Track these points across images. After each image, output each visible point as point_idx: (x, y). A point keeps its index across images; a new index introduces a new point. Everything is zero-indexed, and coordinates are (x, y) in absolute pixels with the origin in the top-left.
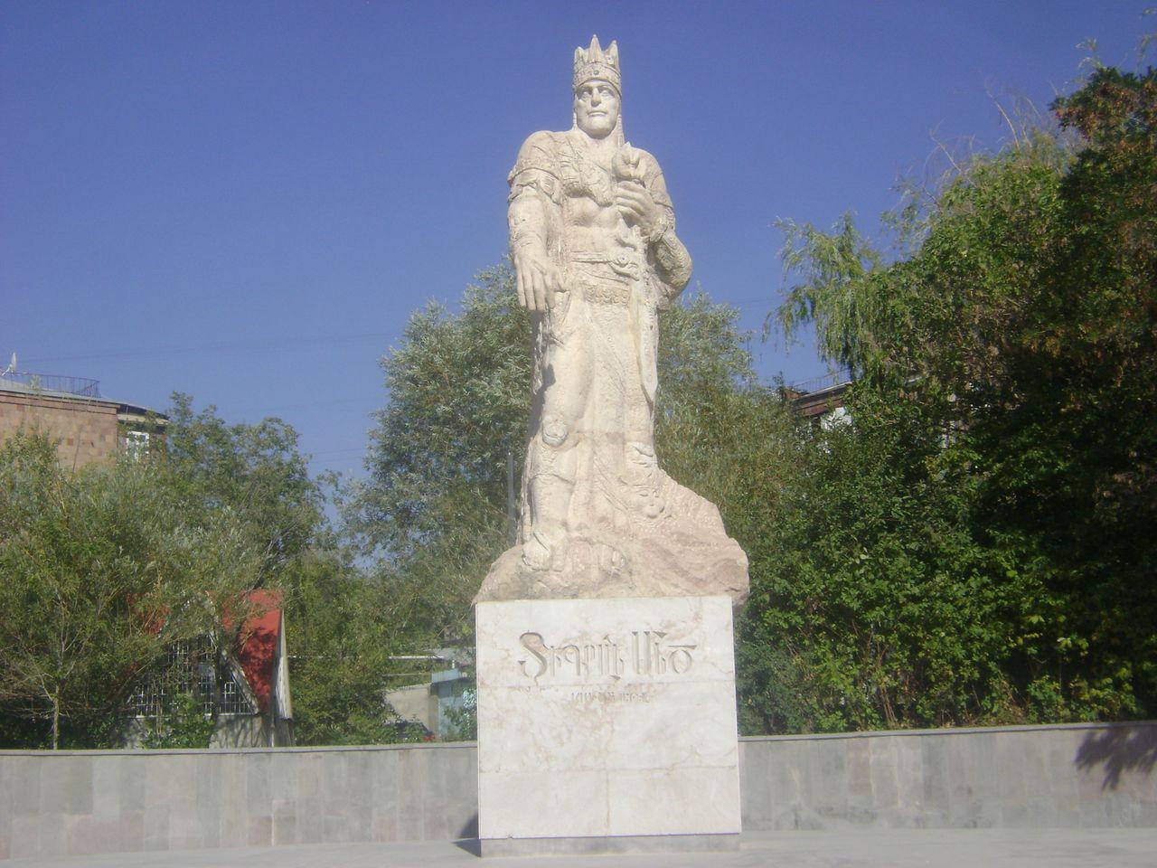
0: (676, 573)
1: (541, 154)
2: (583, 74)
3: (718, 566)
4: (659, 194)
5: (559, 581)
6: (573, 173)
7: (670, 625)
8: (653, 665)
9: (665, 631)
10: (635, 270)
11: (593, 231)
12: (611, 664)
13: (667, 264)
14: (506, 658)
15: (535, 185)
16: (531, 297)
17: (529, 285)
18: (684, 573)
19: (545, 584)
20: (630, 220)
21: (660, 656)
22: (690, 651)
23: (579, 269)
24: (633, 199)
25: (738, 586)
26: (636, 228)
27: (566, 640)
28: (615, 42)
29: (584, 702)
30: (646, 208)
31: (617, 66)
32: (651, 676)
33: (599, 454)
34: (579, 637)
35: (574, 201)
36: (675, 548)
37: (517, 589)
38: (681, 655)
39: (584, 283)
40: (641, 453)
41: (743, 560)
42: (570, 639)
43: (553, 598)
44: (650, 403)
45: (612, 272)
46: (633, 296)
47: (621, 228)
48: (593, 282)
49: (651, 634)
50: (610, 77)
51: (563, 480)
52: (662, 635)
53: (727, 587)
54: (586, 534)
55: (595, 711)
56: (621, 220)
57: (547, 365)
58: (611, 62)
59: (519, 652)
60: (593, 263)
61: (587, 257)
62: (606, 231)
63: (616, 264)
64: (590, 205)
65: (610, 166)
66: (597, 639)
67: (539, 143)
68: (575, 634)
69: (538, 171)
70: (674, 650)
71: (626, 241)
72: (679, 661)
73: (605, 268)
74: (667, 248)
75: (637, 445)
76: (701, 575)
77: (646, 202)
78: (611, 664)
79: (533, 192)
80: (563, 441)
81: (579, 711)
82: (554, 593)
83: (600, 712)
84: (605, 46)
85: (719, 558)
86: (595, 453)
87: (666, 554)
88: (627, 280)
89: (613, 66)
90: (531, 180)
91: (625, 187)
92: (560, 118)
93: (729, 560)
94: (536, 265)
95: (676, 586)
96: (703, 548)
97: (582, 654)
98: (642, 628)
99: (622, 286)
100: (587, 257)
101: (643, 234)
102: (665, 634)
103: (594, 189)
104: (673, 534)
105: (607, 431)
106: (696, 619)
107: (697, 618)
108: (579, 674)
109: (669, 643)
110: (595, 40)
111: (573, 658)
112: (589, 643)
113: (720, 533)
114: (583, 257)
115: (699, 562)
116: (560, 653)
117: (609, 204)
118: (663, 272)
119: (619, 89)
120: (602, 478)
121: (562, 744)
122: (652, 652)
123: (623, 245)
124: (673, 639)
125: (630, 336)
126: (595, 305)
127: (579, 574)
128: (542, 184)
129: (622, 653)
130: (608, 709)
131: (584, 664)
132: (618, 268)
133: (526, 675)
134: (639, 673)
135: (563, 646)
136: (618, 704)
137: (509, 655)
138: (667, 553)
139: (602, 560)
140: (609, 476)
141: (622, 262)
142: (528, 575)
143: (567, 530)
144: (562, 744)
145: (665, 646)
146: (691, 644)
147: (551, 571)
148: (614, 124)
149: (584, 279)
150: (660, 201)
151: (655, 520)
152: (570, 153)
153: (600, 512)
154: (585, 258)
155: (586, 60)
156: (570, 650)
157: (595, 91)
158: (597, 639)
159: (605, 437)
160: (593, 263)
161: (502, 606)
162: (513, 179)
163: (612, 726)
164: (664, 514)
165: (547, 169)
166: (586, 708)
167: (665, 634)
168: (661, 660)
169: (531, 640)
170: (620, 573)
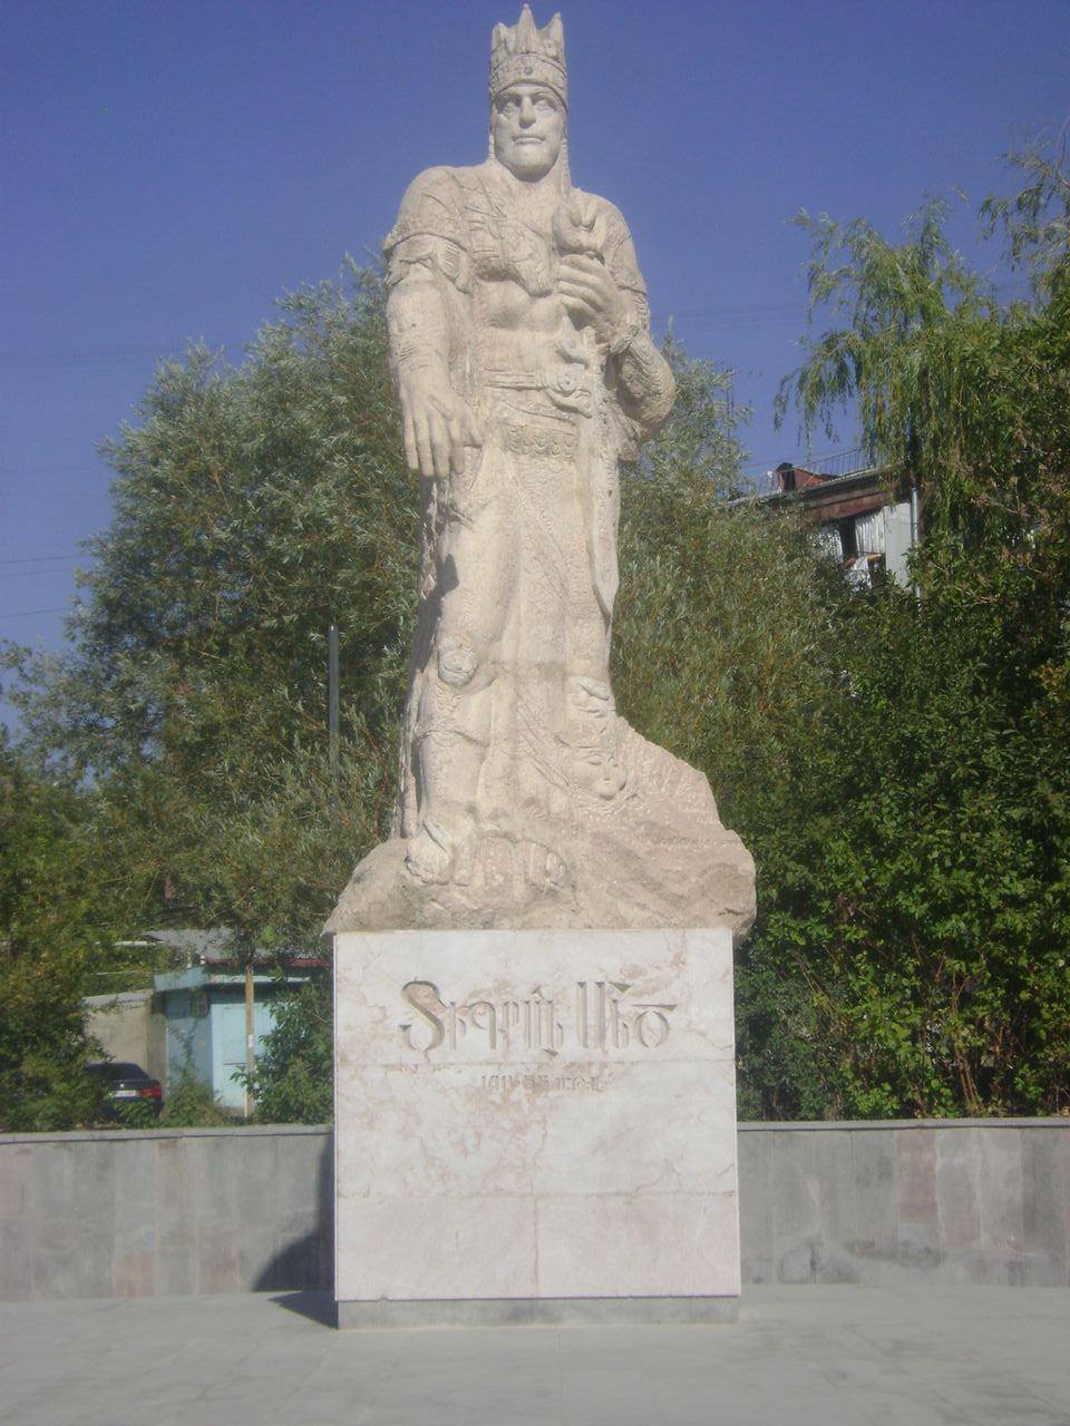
0: (644, 885)
1: (439, 210)
2: (507, 73)
3: (707, 876)
4: (625, 272)
5: (464, 900)
6: (490, 242)
7: (635, 972)
8: (609, 1034)
9: (628, 982)
10: (585, 401)
11: (521, 336)
12: (544, 1031)
13: (636, 389)
14: (381, 1021)
15: (429, 262)
16: (427, 454)
17: (424, 436)
18: (654, 886)
19: (442, 904)
20: (579, 319)
21: (620, 1021)
22: (666, 1014)
23: (497, 399)
24: (581, 283)
25: (738, 905)
26: (589, 331)
27: (473, 994)
28: (558, 15)
29: (501, 1090)
30: (606, 300)
31: (562, 59)
32: (606, 1052)
33: (525, 696)
36: (642, 847)
37: (398, 912)
38: (652, 1020)
39: (505, 422)
40: (591, 694)
41: (748, 866)
42: (480, 992)
43: (454, 927)
44: (605, 615)
46: (583, 444)
47: (565, 333)
48: (520, 420)
49: (607, 986)
50: (551, 79)
51: (470, 740)
52: (623, 987)
53: (722, 909)
54: (505, 825)
55: (518, 1104)
56: (566, 320)
57: (444, 554)
58: (552, 52)
59: (401, 1012)
60: (520, 389)
62: (541, 336)
63: (557, 392)
64: (517, 295)
65: (548, 229)
66: (523, 992)
67: (434, 185)
68: (489, 984)
69: (434, 238)
70: (641, 1011)
71: (573, 353)
73: (538, 397)
74: (636, 362)
75: (585, 681)
76: (681, 889)
77: (606, 289)
78: (544, 1031)
80: (471, 678)
81: (492, 1102)
82: (457, 920)
83: (525, 1105)
84: (542, 21)
85: (710, 861)
86: (519, 696)
87: (629, 855)
88: (573, 417)
89: (556, 59)
90: (419, 255)
91: (574, 265)
92: (468, 146)
93: (725, 865)
94: (435, 403)
95: (643, 907)
97: (499, 1016)
99: (566, 428)
101: (599, 340)
102: (628, 986)
103: (523, 267)
104: (639, 824)
105: (539, 659)
107: (679, 961)
108: (493, 1046)
110: (526, 13)
111: (484, 1021)
112: (511, 999)
113: (711, 822)
114: (504, 379)
115: (680, 868)
116: (465, 1014)
117: (545, 294)
118: (629, 401)
119: (564, 97)
120: (530, 736)
121: (466, 1154)
122: (608, 1014)
123: (569, 359)
124: (640, 994)
128: (441, 261)
129: (561, 1015)
130: (538, 1101)
131: (501, 1030)
132: (559, 398)
133: (410, 1046)
134: (586, 1046)
136: (552, 1094)
140: (542, 732)
141: (567, 388)
142: (415, 890)
143: (477, 819)
144: (466, 1154)
145: (627, 1006)
147: (452, 886)
148: (554, 157)
149: (506, 415)
150: (627, 284)
151: (611, 803)
152: (485, 208)
154: (508, 381)
155: (511, 46)
156: (480, 1009)
157: (527, 101)
158: (523, 992)
160: (520, 389)
162: (393, 248)
163: (544, 1128)
164: (626, 792)
166: (505, 1099)
167: (628, 986)
168: (620, 1026)
169: (420, 992)
170: (558, 888)
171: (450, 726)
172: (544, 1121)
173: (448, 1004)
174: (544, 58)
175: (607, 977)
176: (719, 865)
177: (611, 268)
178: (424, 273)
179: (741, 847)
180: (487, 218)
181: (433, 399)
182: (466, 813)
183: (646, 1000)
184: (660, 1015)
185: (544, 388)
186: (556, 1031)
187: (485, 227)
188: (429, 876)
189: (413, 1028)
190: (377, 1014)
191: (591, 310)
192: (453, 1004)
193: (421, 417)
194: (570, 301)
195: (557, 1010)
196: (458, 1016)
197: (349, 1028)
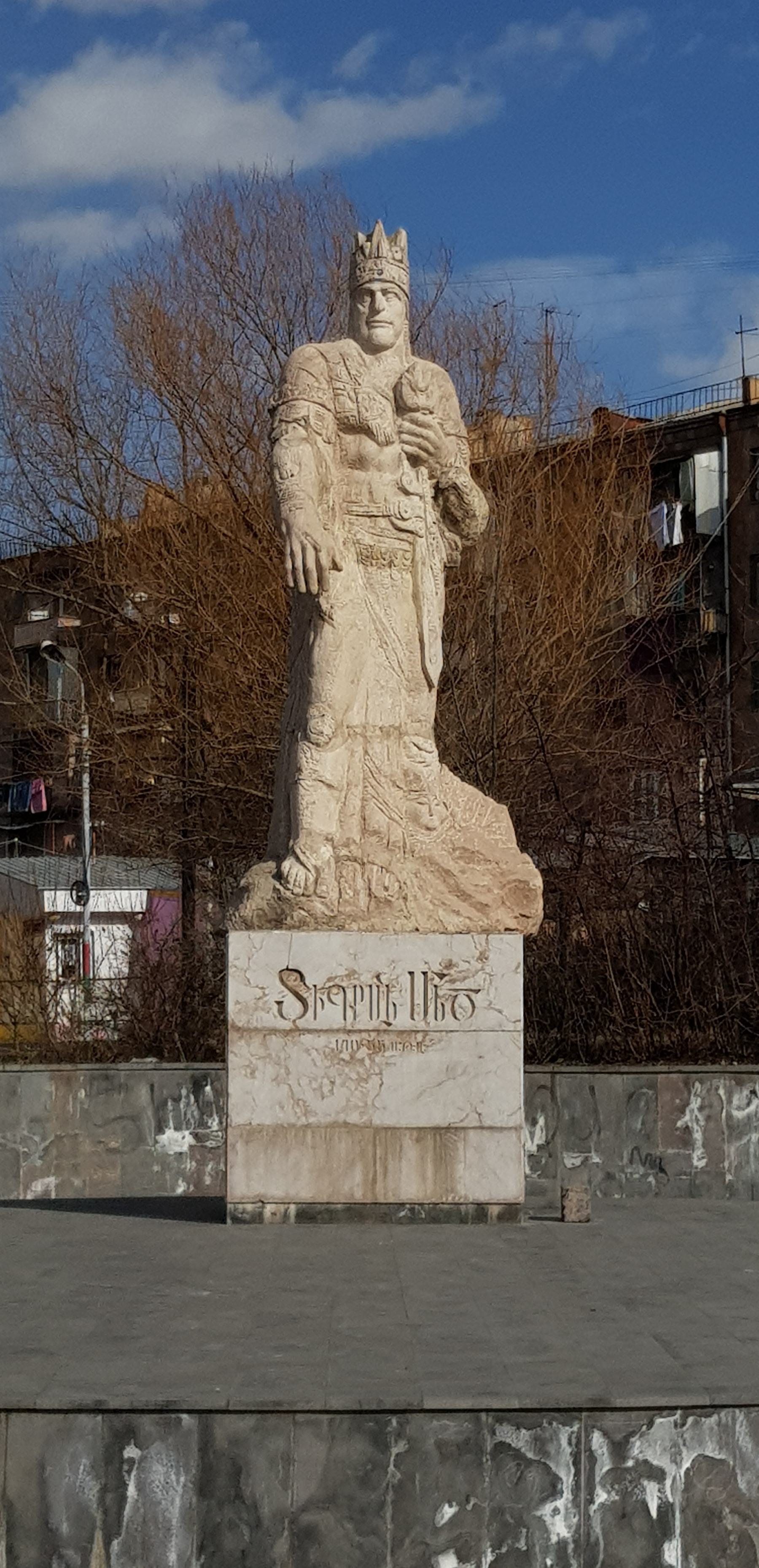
0: (458, 896)
1: (311, 380)
4: (451, 423)
5: (323, 908)
6: (350, 405)
9: (445, 972)
11: (372, 475)
13: (459, 514)
15: (303, 423)
19: (308, 912)
20: (415, 461)
21: (439, 1000)
22: (473, 996)
26: (424, 470)
27: (329, 980)
29: (350, 1050)
30: (436, 448)
31: (406, 260)
33: (370, 752)
34: (346, 976)
35: (349, 438)
37: (275, 917)
38: (462, 1000)
41: (538, 882)
42: (336, 977)
43: (316, 929)
45: (391, 527)
49: (430, 975)
50: (397, 278)
55: (362, 1061)
56: (406, 463)
58: (398, 256)
59: (277, 991)
61: (362, 510)
62: (388, 477)
63: (398, 519)
64: (370, 446)
66: (367, 978)
68: (342, 972)
69: (307, 403)
70: (454, 994)
71: (411, 489)
72: (461, 1007)
73: (383, 523)
74: (459, 494)
79: (302, 432)
81: (343, 1060)
83: (367, 1062)
88: (410, 538)
89: (401, 261)
90: (296, 416)
91: (414, 422)
93: (520, 881)
96: (490, 867)
100: (362, 510)
101: (431, 477)
102: (445, 975)
103: (373, 424)
107: (483, 957)
109: (448, 986)
111: (338, 999)
112: (356, 982)
119: (407, 291)
123: (407, 493)
124: (453, 981)
126: (370, 569)
130: (377, 1059)
131: (351, 1007)
133: (282, 1016)
134: (413, 1019)
136: (387, 1054)
138: (448, 872)
140: (383, 779)
141: (406, 516)
148: (397, 336)
150: (452, 432)
151: (435, 833)
155: (367, 251)
156: (335, 990)
159: (378, 732)
160: (370, 517)
161: (257, 936)
163: (381, 1079)
166: (352, 1057)
167: (445, 975)
168: (439, 1006)
170: (393, 900)
171: (314, 776)
172: (381, 1073)
173: (311, 986)
174: (392, 261)
175: (429, 969)
176: (515, 881)
177: (440, 421)
179: (532, 866)
181: (307, 535)
184: (468, 996)
186: (391, 1007)
187: (345, 393)
189: (284, 1004)
190: (259, 993)
191: (423, 454)
192: (315, 986)
193: (297, 549)
194: (408, 448)
196: (318, 995)
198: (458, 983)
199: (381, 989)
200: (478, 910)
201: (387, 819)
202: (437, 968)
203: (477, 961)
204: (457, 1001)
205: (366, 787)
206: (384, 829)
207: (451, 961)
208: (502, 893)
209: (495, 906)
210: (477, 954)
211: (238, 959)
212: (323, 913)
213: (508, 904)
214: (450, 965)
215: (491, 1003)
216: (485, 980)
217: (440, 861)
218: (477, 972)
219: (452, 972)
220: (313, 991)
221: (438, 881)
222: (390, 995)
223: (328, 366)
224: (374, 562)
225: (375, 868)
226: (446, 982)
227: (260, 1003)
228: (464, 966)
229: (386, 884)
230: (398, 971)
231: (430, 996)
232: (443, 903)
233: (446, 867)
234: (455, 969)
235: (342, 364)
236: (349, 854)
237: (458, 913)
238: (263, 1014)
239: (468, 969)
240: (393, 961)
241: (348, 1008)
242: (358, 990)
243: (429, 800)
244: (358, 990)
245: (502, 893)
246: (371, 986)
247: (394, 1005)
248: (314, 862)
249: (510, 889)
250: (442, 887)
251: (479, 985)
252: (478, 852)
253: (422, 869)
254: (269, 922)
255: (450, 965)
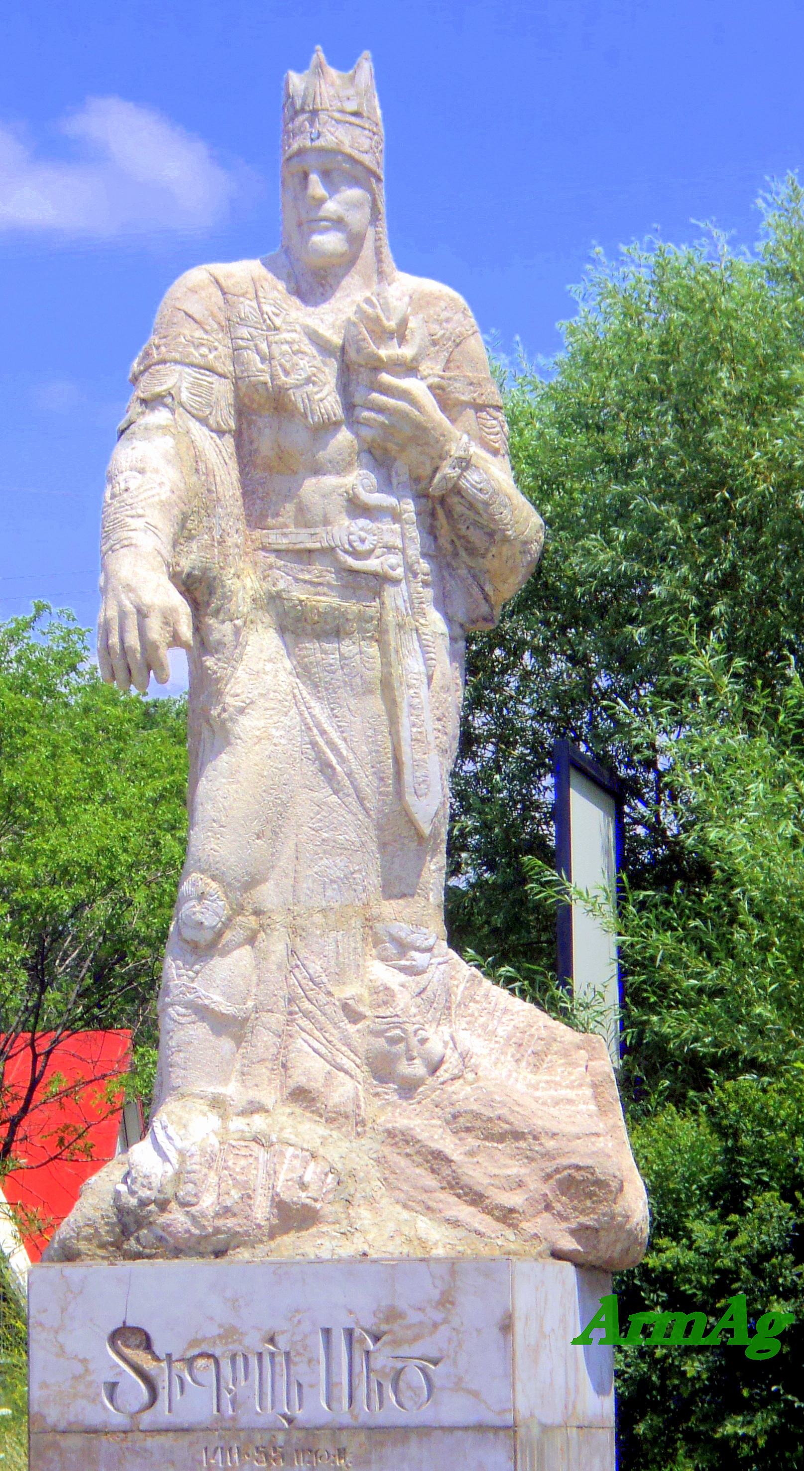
0: (459, 1196)
5: (189, 1225)
9: (384, 1327)
14: (80, 1376)
15: (169, 400)
27: (194, 1343)
28: (367, 54)
33: (303, 952)
34: (219, 1335)
46: (391, 618)
48: (298, 593)
49: (358, 1332)
53: (574, 1225)
63: (346, 552)
66: (253, 1341)
68: (213, 1330)
70: (399, 1365)
72: (409, 1387)
86: (293, 952)
90: (158, 389)
93: (578, 1168)
98: (340, 1323)
102: (385, 1333)
106: (443, 1305)
109: (388, 1351)
120: (307, 1005)
124: (396, 1343)
125: (376, 704)
127: (227, 1211)
128: (185, 396)
129: (300, 1369)
132: (351, 561)
135: (189, 1354)
137: (87, 1370)
138: (439, 1156)
139: (282, 1177)
141: (361, 547)
143: (224, 1117)
145: (383, 1359)
146: (434, 1353)
149: (281, 585)
152: (254, 317)
153: (298, 1078)
154: (284, 543)
156: (201, 1362)
165: (199, 360)
167: (385, 1333)
170: (318, 1205)
173: (163, 1356)
174: (337, 115)
175: (357, 1323)
176: (569, 1167)
178: (161, 416)
180: (254, 332)
182: (206, 1108)
183: (405, 1351)
184: (423, 1370)
185: (333, 549)
188: (145, 1193)
190: (79, 1369)
192: (169, 1356)
195: (296, 1364)
197: (44, 1385)
198: (406, 1346)
199: (277, 1359)
200: (498, 1219)
201: (328, 1067)
202: (368, 1321)
203: (436, 1307)
204: (402, 1377)
205: (291, 1013)
206: (317, 1085)
207: (392, 1308)
208: (546, 1189)
209: (531, 1210)
210: (436, 1294)
211: (45, 1311)
212: (187, 1231)
213: (558, 1206)
214: (393, 1315)
215: (460, 1379)
216: (450, 1340)
217: (423, 1136)
218: (435, 1325)
219: (395, 1327)
220: (164, 1365)
221: (418, 1171)
222: (293, 1368)
223: (226, 302)
224: (309, 628)
225: (290, 1151)
226: (385, 1344)
227: (81, 1388)
228: (414, 1317)
229: (306, 1179)
230: (306, 1327)
231: (356, 1369)
232: (428, 1208)
233: (435, 1146)
234: (400, 1321)
235: (252, 295)
236: (246, 1128)
237: (455, 1223)
238: (83, 1402)
239: (421, 1323)
240: (297, 1311)
241: (224, 1392)
242: (240, 1361)
243: (404, 1031)
244: (240, 1361)
245: (546, 1189)
246: (260, 1355)
247: (300, 1385)
248: (179, 1144)
249: (560, 1182)
250: (431, 1181)
251: (441, 1350)
252: (499, 1118)
253: (387, 1150)
254: (102, 1246)
255: (393, 1315)
